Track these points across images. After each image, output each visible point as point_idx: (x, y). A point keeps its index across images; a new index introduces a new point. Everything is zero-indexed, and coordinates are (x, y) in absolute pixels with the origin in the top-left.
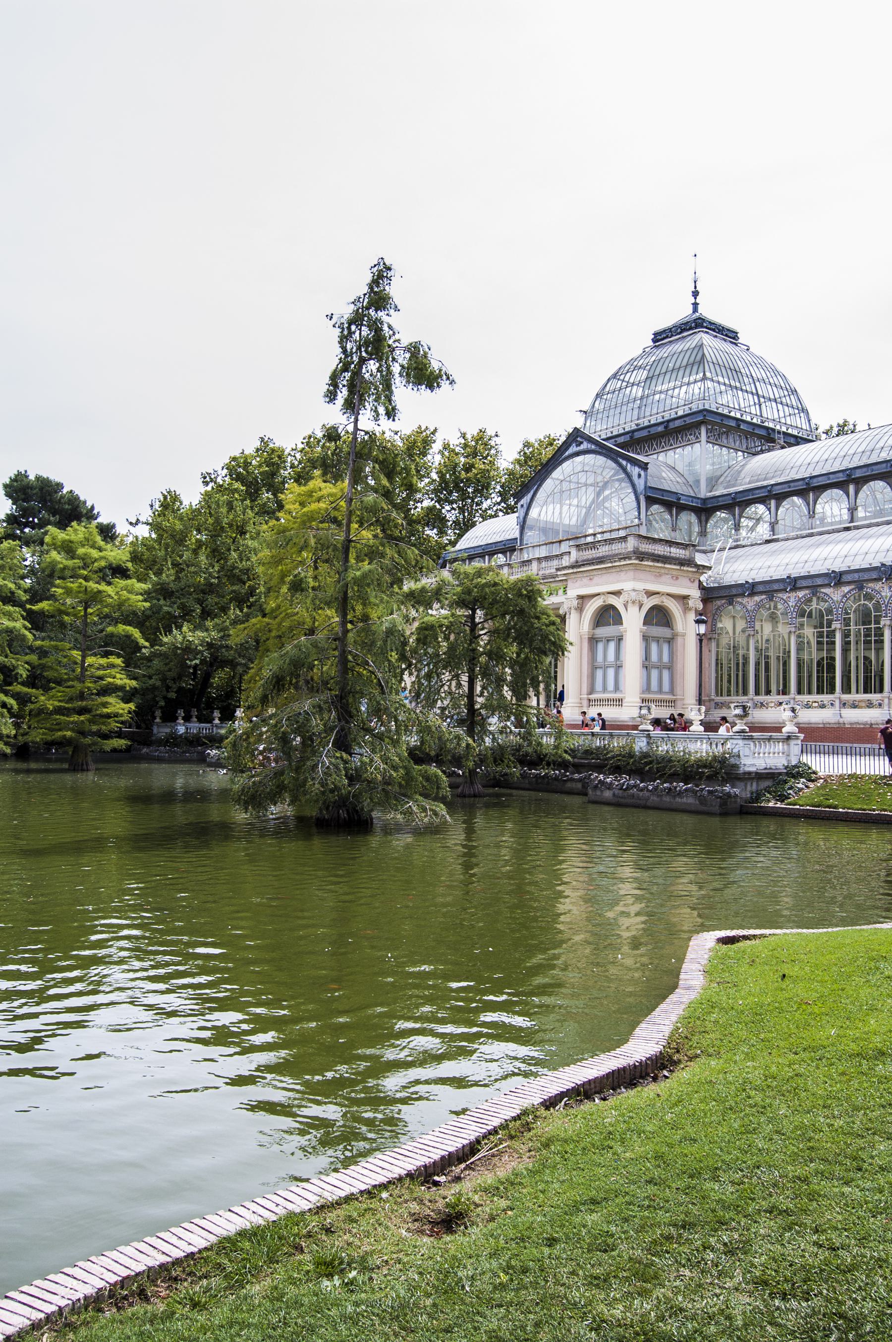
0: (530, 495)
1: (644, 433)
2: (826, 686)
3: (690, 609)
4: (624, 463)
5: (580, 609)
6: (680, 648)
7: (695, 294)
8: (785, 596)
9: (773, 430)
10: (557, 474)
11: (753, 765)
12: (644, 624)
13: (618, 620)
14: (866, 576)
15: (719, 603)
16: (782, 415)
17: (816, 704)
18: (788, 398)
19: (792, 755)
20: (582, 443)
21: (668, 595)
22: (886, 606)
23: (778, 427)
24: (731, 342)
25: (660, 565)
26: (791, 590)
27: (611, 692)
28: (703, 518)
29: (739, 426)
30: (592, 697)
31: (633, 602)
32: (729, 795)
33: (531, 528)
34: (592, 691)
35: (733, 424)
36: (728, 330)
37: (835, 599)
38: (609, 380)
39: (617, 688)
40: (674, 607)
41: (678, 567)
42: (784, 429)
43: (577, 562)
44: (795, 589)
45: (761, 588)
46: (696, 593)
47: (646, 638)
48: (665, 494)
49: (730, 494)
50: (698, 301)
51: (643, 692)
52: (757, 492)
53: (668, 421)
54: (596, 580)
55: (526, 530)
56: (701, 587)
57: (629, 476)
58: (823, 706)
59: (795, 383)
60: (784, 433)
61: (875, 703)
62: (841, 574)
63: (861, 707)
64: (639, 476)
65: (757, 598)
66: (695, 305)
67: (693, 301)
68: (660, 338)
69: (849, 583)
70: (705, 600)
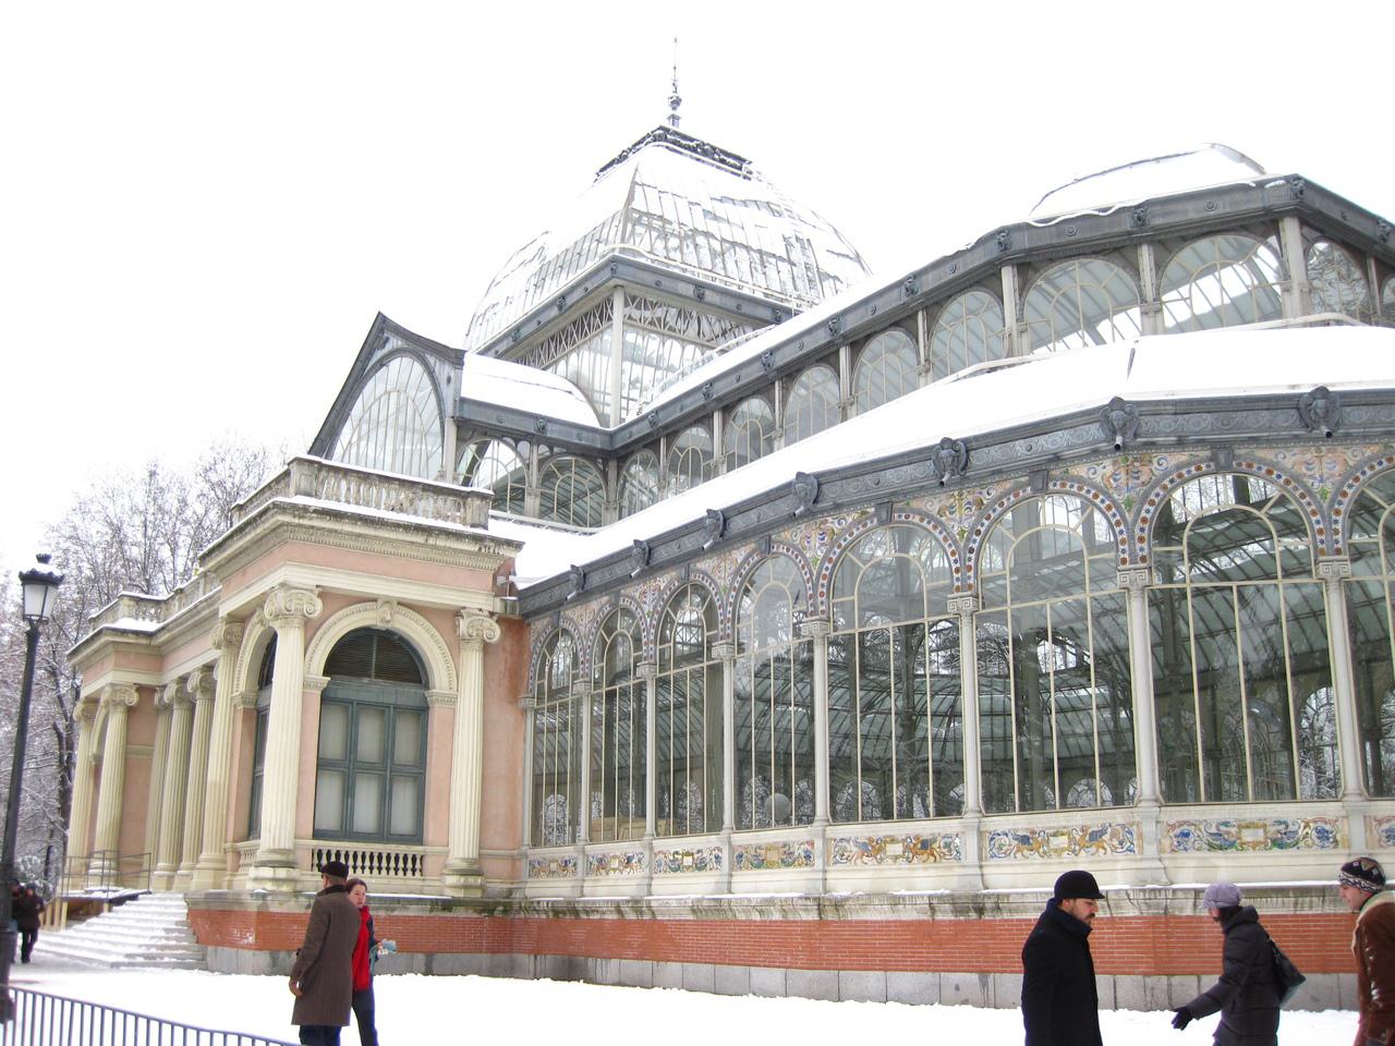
3: (468, 639)
4: (431, 360)
14: (769, 513)
17: (688, 861)
20: (387, 340)
22: (815, 586)
35: (689, 290)
37: (721, 583)
50: (676, 113)
52: (689, 400)
58: (700, 866)
61: (799, 851)
63: (770, 865)
64: (449, 380)
65: (595, 605)
69: (744, 537)
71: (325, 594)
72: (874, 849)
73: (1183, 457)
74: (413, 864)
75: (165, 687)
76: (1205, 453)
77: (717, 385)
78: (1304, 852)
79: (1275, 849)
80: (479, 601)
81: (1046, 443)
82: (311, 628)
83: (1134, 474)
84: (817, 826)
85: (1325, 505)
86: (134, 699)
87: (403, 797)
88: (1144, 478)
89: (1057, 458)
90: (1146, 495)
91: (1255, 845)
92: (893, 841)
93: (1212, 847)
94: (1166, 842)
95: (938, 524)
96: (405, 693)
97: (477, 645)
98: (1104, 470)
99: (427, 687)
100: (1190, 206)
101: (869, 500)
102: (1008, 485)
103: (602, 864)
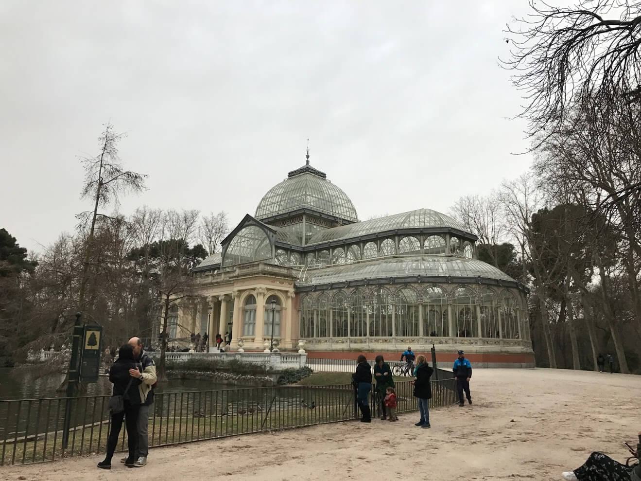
0: (227, 244)
1: (280, 217)
2: (323, 333)
5: (239, 297)
6: (284, 314)
7: (308, 157)
8: (328, 292)
9: (337, 218)
10: (240, 234)
11: (280, 367)
12: (267, 303)
13: (255, 302)
15: (302, 294)
16: (342, 211)
17: (340, 342)
18: (346, 204)
19: (302, 362)
20: (250, 221)
23: (340, 217)
26: (330, 289)
27: (250, 335)
28: (303, 256)
29: (321, 216)
30: (244, 337)
31: (260, 294)
32: (267, 380)
33: (228, 258)
34: (243, 334)
36: (321, 173)
38: (268, 192)
39: (253, 334)
40: (281, 296)
41: (283, 278)
42: (343, 218)
43: (238, 274)
44: (332, 289)
45: (318, 288)
46: (292, 290)
47: (266, 310)
48: (284, 245)
49: (313, 246)
50: (309, 159)
51: (264, 335)
53: (290, 212)
54: (246, 283)
55: (225, 259)
56: (295, 287)
57: (268, 237)
59: (350, 198)
60: (343, 219)
62: (350, 282)
64: (273, 236)
65: (317, 293)
66: (308, 161)
67: (307, 160)
68: (291, 175)
70: (296, 293)
72: (377, 341)
73: (428, 284)
76: (432, 284)
81: (408, 280)
82: (264, 295)
89: (409, 282)
92: (381, 340)
95: (389, 290)
98: (416, 285)
99: (281, 306)
101: (377, 284)
103: (320, 342)
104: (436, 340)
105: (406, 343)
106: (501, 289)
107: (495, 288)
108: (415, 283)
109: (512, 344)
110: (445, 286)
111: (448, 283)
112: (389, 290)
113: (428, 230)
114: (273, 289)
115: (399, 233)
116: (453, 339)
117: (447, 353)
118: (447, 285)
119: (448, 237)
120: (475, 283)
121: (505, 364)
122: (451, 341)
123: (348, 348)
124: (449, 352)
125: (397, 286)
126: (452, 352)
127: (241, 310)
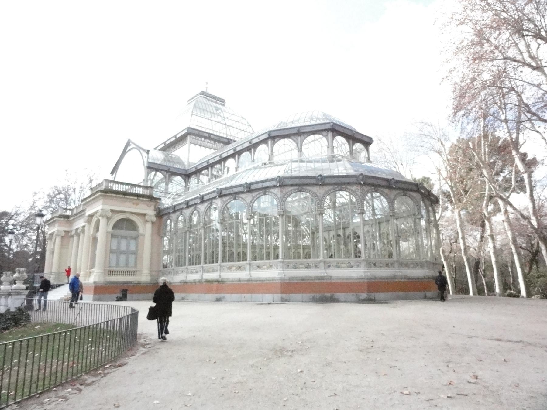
17: (194, 271)
21: (132, 213)
24: (221, 104)
25: (121, 196)
28: (187, 180)
41: (136, 198)
58: (197, 272)
69: (207, 200)
71: (112, 211)
72: (230, 268)
73: (292, 188)
74: (134, 273)
75: (72, 231)
76: (297, 187)
77: (210, 161)
78: (312, 269)
79: (306, 269)
80: (151, 212)
82: (108, 218)
83: (281, 191)
84: (219, 263)
85: (320, 199)
86: (63, 234)
87: (132, 258)
88: (284, 192)
89: (267, 188)
90: (284, 196)
91: (302, 268)
92: (233, 266)
93: (293, 268)
94: (284, 267)
95: (244, 200)
96: (132, 233)
97: (151, 222)
98: (276, 191)
99: (138, 232)
100: (309, 127)
102: (257, 193)
103: (177, 273)
104: (302, 264)
105: (262, 269)
106: (395, 192)
107: (386, 191)
108: (274, 187)
109: (412, 266)
110: (314, 189)
111: (317, 185)
112: (244, 200)
113: (306, 128)
114: (124, 212)
115: (273, 134)
116: (324, 262)
117: (316, 281)
118: (318, 188)
119: (330, 134)
120: (356, 184)
121: (401, 294)
122: (322, 264)
123: (249, 277)
124: (319, 279)
125: (255, 194)
126: (324, 279)
127: (91, 238)
